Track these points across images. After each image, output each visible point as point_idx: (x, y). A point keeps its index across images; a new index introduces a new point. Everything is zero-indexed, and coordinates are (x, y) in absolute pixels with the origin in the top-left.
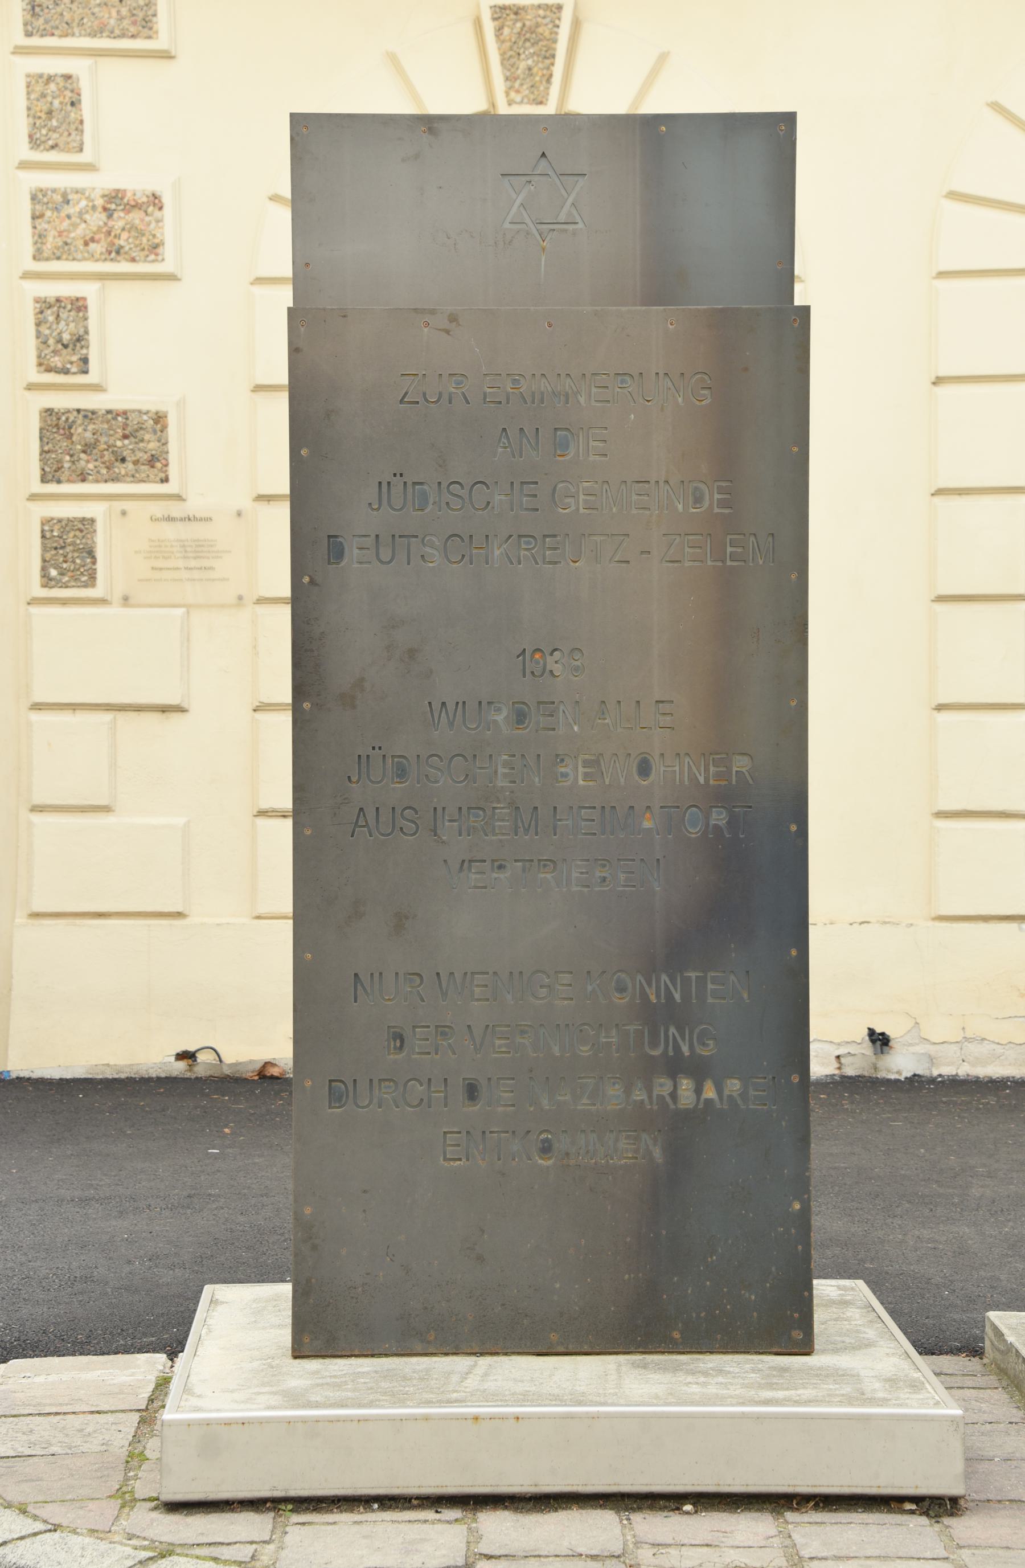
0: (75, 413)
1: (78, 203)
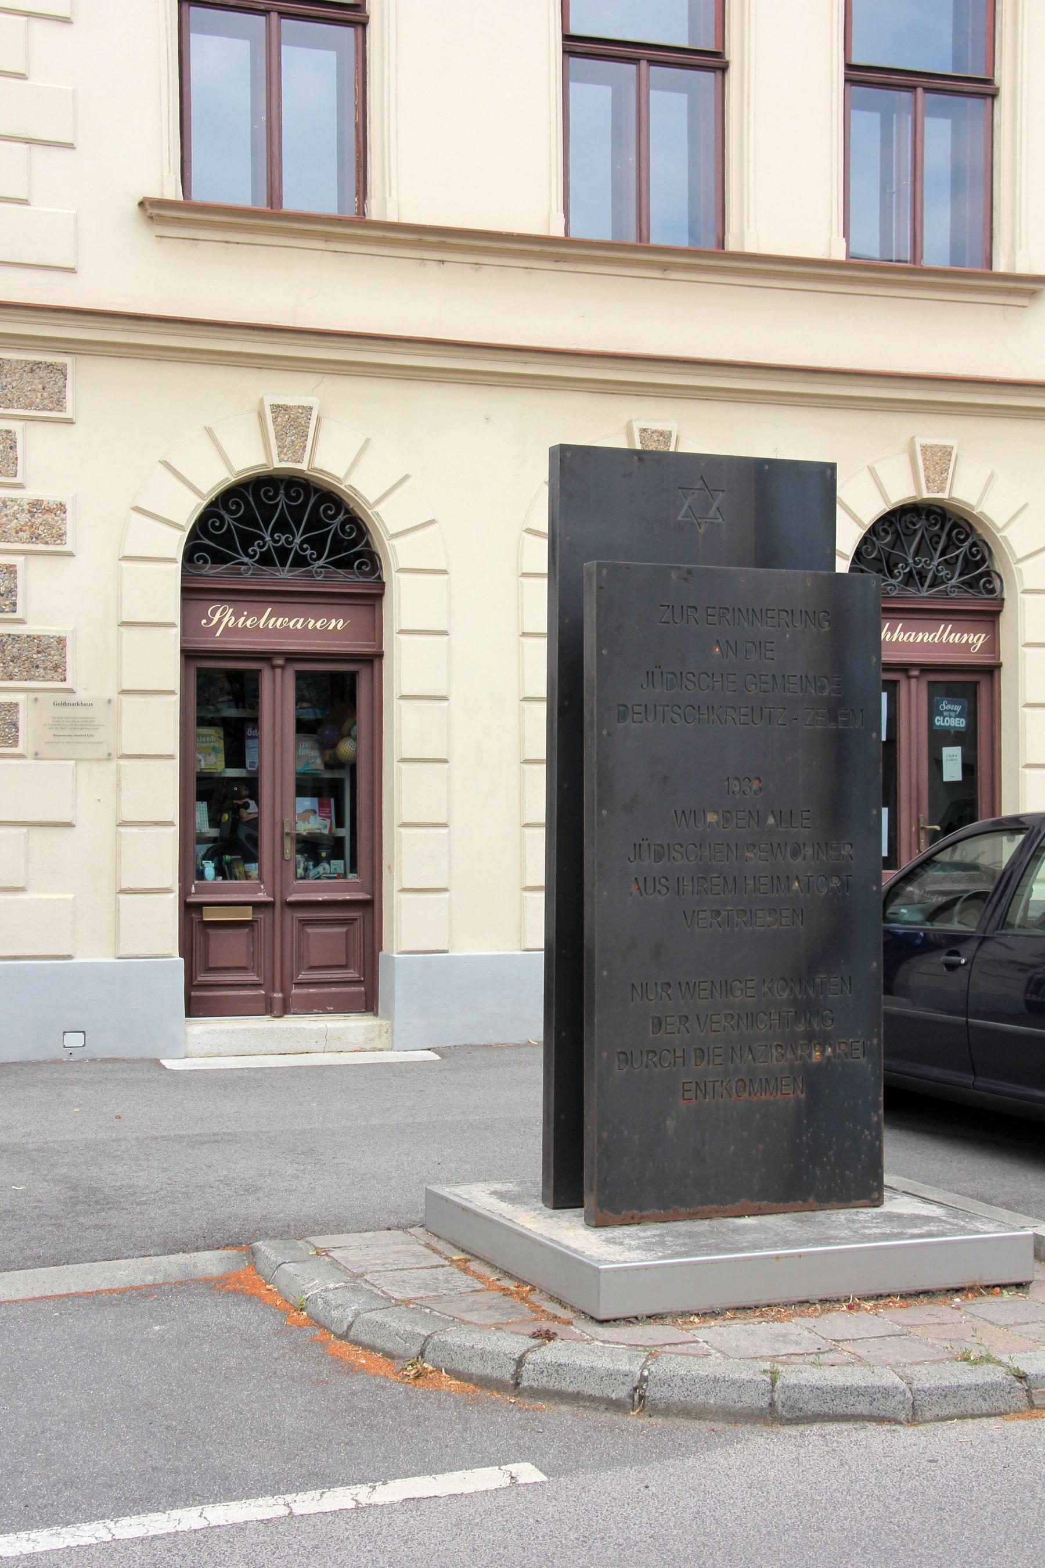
0: (7, 637)
1: (12, 508)
